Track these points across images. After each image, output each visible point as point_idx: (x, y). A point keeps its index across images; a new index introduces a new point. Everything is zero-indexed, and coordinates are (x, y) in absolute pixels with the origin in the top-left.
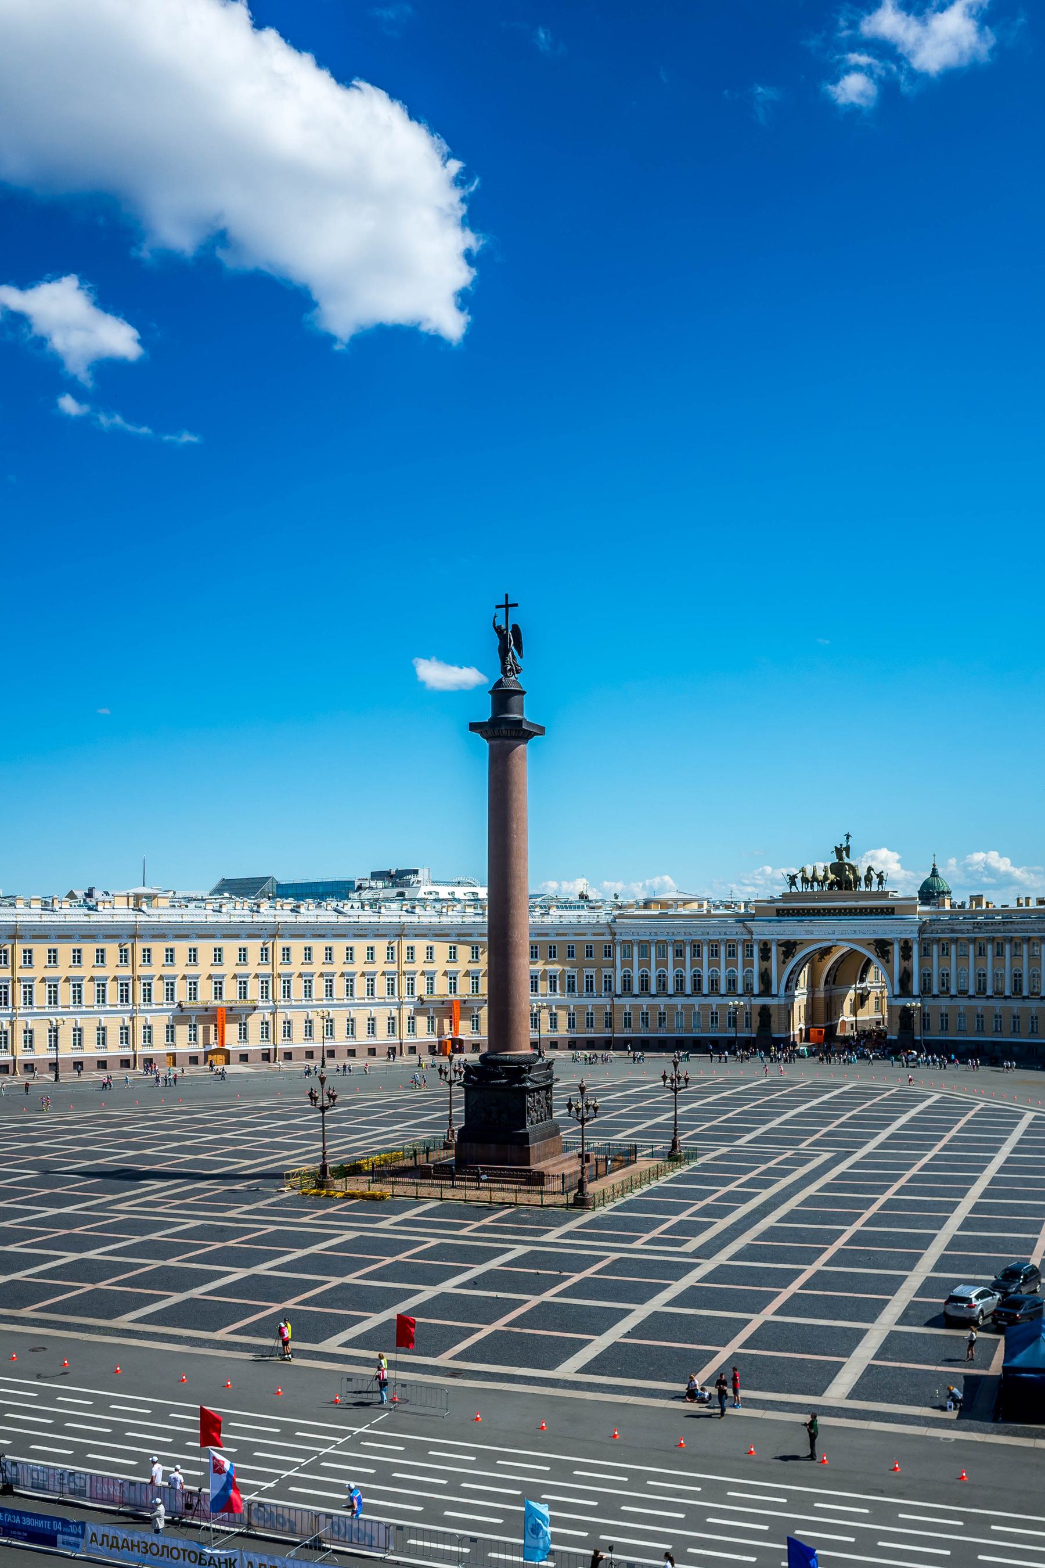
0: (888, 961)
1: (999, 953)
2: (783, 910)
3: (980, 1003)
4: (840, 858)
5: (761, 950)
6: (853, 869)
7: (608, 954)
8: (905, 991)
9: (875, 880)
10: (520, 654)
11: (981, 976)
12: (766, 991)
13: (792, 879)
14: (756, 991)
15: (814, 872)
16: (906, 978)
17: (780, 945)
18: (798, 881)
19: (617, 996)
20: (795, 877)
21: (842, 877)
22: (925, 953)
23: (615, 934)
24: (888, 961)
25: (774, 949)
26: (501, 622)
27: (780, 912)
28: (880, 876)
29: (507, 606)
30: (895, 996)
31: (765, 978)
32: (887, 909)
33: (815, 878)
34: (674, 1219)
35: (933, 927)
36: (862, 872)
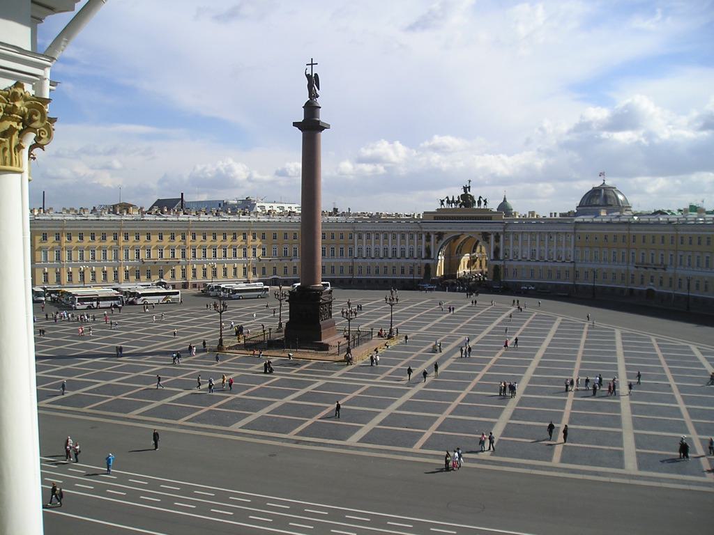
0: (488, 243)
6: (472, 197)
9: (483, 203)
10: (319, 89)
12: (428, 257)
14: (423, 257)
16: (497, 251)
18: (445, 203)
20: (444, 200)
21: (467, 200)
24: (488, 243)
25: (432, 236)
26: (309, 72)
28: (485, 201)
29: (312, 64)
31: (428, 250)
33: (453, 201)
34: (395, 368)
36: (477, 200)
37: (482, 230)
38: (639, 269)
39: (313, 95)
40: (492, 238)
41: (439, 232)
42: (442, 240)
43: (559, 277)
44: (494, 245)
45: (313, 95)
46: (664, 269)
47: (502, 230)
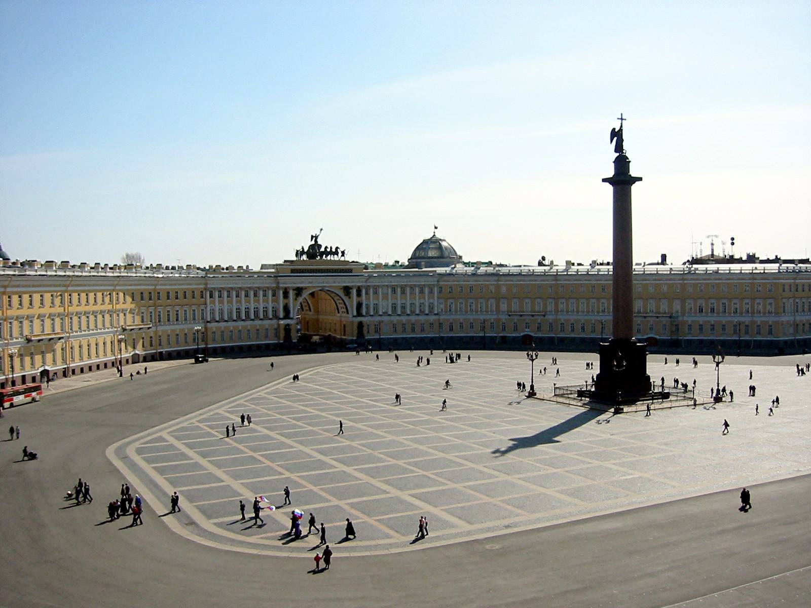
0: (350, 298)
1: (403, 292)
2: (294, 270)
3: (395, 319)
4: (316, 241)
5: (283, 293)
7: (202, 297)
8: (359, 314)
11: (394, 307)
12: (287, 315)
13: (297, 251)
14: (281, 316)
17: (294, 290)
19: (208, 322)
24: (350, 298)
27: (293, 271)
28: (343, 253)
30: (354, 316)
36: (334, 250)
37: (345, 285)
38: (512, 317)
39: (619, 148)
40: (354, 292)
42: (301, 296)
43: (423, 330)
44: (356, 299)
45: (619, 148)
46: (544, 316)
47: (364, 284)
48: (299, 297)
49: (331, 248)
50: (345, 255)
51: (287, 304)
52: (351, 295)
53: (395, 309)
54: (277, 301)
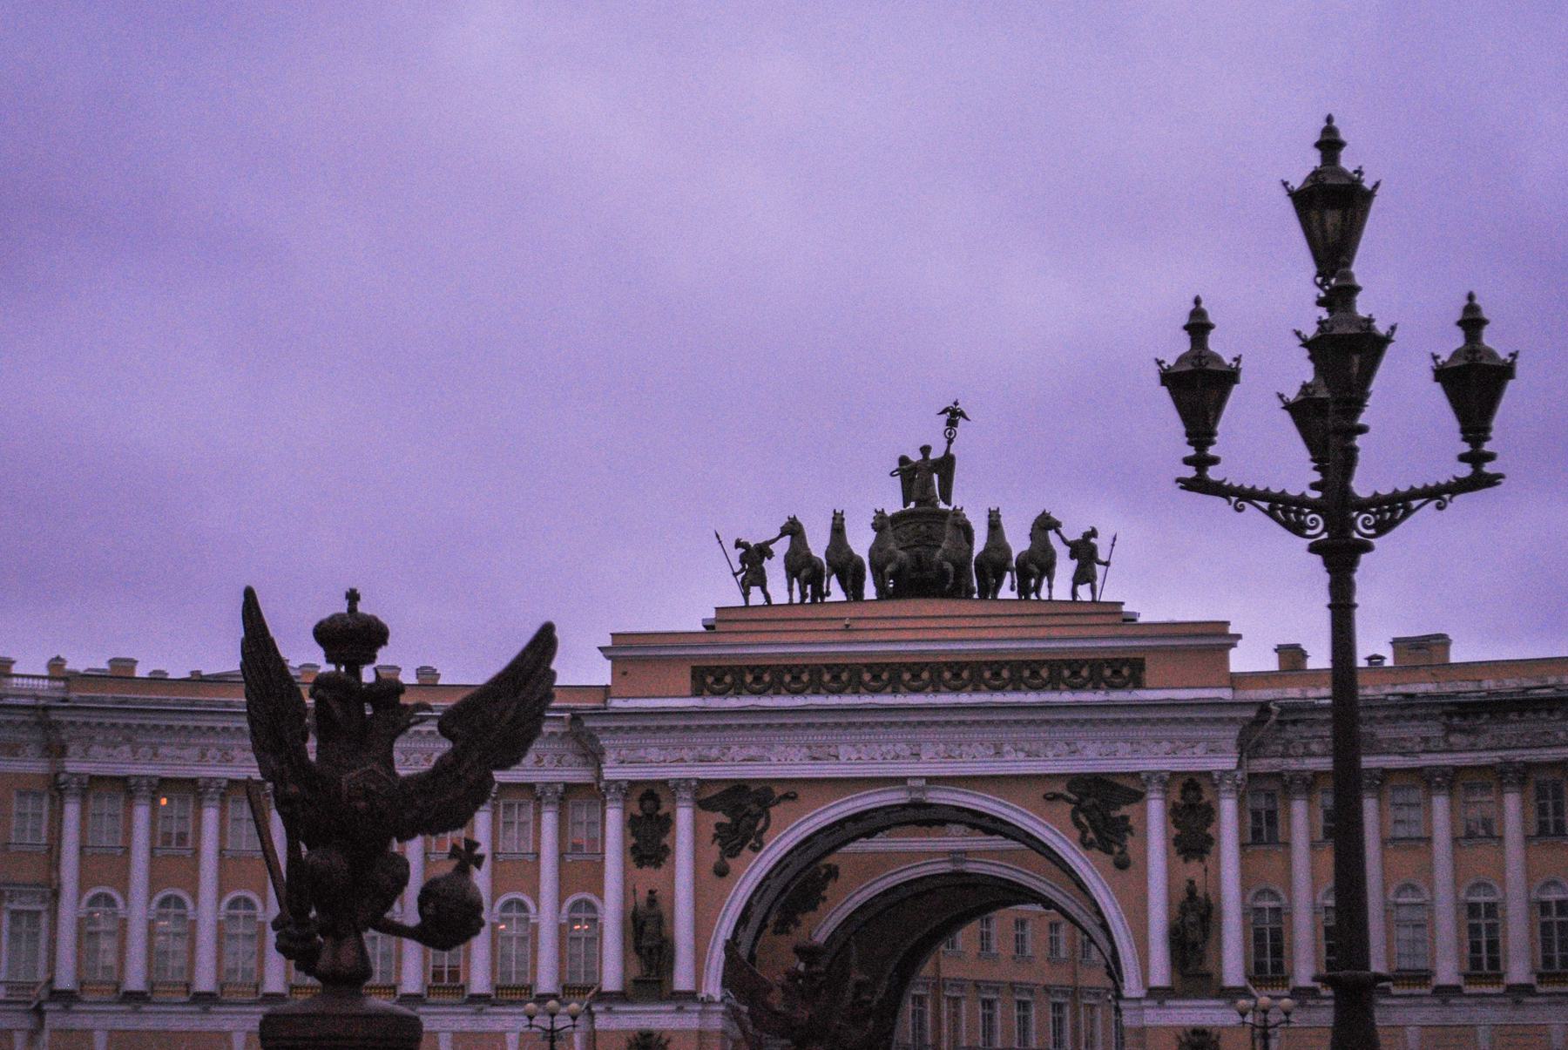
4: (925, 500)
9: (1065, 568)
14: (611, 979)
15: (838, 529)
17: (703, 804)
18: (775, 570)
20: (763, 551)
22: (1263, 832)
23: (55, 750)
24: (1122, 865)
25: (684, 816)
27: (707, 678)
28: (1084, 552)
32: (1116, 665)
35: (1290, 732)
36: (1018, 542)
41: (738, 789)
48: (746, 851)
49: (994, 525)
50: (1099, 569)
51: (652, 900)
52: (1131, 842)
53: (1475, 948)
54: (596, 882)
